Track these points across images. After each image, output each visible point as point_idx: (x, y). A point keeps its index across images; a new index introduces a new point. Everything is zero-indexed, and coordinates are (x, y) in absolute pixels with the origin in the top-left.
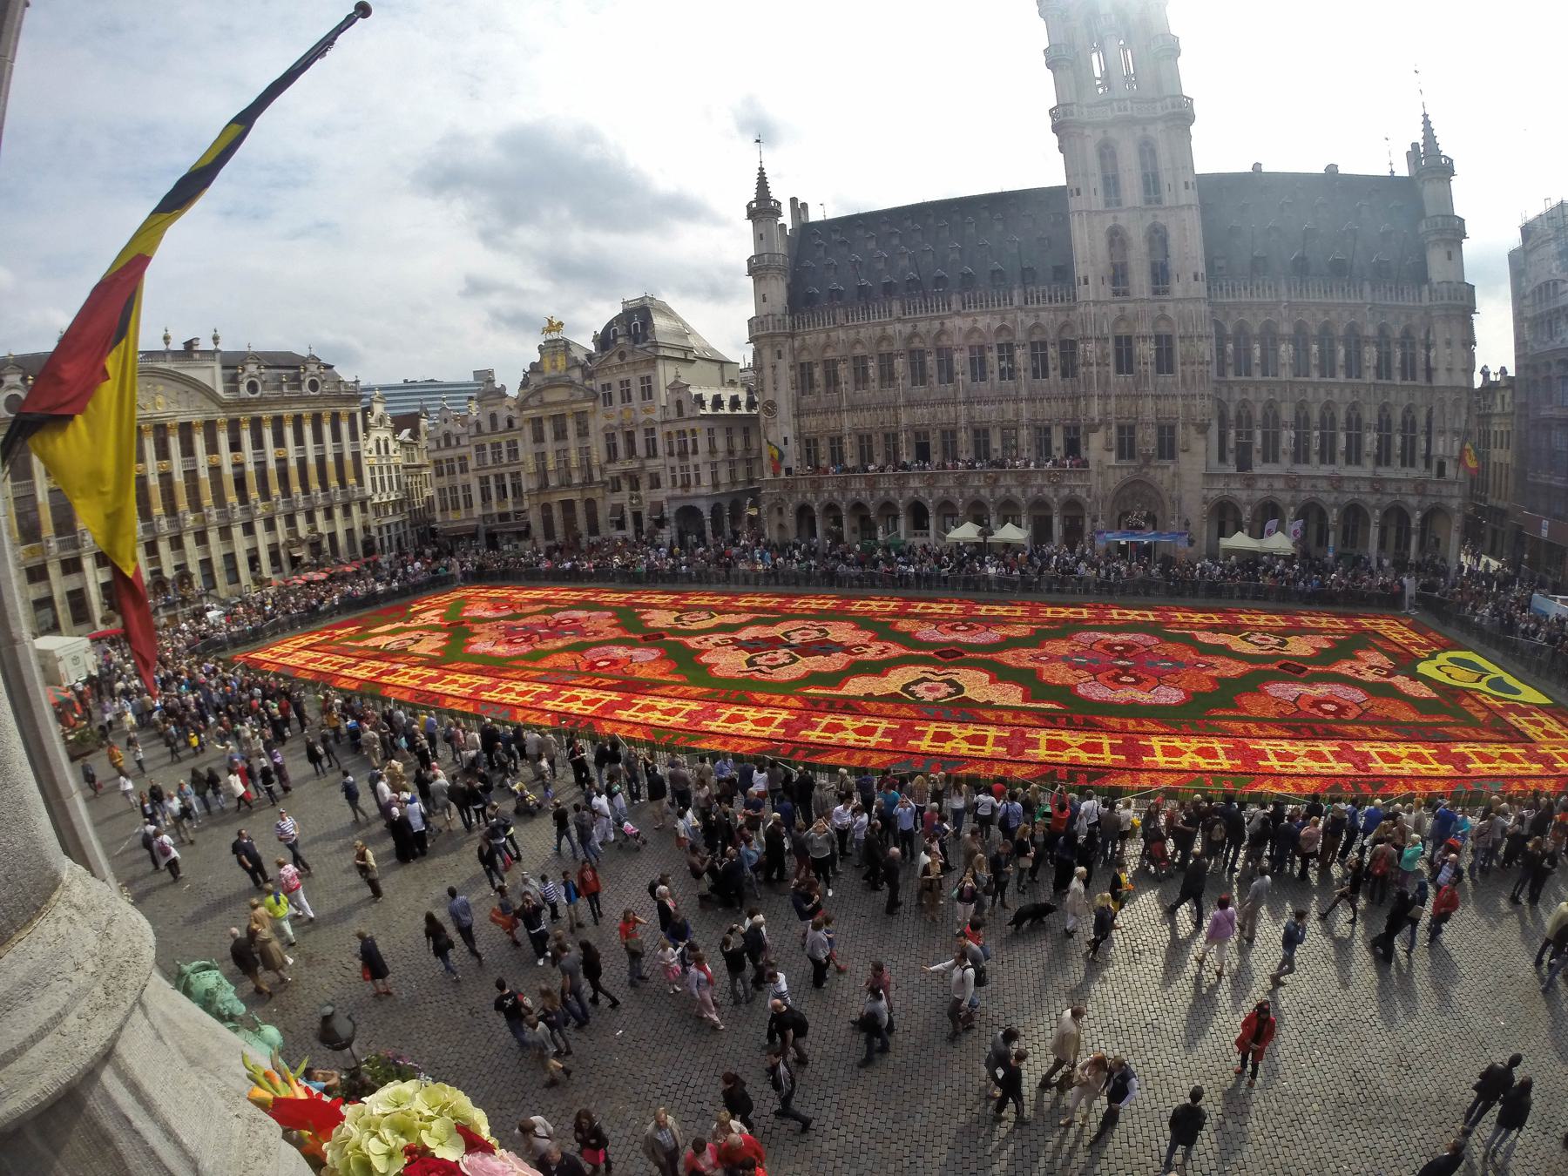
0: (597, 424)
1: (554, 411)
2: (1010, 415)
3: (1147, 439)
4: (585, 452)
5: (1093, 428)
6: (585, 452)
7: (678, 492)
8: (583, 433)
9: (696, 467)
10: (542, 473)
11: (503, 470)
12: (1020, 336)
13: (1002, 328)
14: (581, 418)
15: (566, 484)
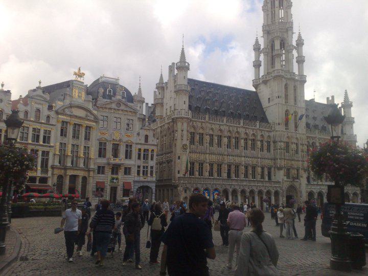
0: (95, 136)
1: (77, 121)
2: (255, 163)
3: (293, 172)
4: (87, 148)
5: (280, 169)
6: (87, 148)
7: (142, 179)
8: (87, 138)
9: (152, 167)
10: (62, 157)
11: (37, 148)
12: (259, 138)
13: (253, 134)
14: (88, 128)
15: (75, 165)
